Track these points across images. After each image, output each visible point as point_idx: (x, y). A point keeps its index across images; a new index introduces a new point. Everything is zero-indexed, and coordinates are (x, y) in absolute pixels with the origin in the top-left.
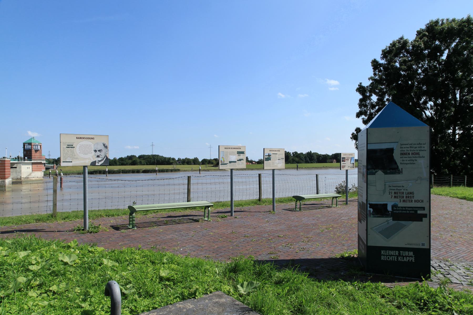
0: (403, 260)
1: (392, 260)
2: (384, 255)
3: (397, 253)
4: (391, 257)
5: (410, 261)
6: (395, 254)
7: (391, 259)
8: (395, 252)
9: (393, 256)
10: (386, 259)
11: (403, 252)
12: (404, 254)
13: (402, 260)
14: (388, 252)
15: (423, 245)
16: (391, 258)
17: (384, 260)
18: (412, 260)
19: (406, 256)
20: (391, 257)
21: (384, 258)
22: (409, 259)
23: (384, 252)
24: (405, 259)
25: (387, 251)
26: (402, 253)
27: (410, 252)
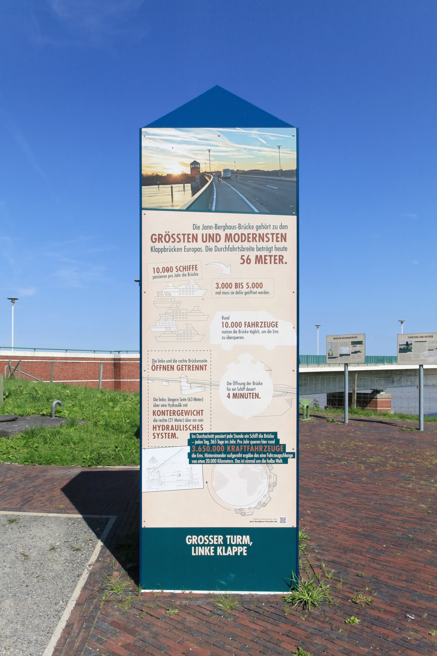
0: (226, 552)
3: (220, 539)
5: (239, 554)
6: (217, 541)
8: (217, 538)
11: (232, 536)
12: (234, 541)
13: (224, 554)
15: (283, 520)
18: (242, 553)
19: (237, 545)
22: (236, 551)
24: (230, 552)
26: (230, 538)
27: (244, 537)
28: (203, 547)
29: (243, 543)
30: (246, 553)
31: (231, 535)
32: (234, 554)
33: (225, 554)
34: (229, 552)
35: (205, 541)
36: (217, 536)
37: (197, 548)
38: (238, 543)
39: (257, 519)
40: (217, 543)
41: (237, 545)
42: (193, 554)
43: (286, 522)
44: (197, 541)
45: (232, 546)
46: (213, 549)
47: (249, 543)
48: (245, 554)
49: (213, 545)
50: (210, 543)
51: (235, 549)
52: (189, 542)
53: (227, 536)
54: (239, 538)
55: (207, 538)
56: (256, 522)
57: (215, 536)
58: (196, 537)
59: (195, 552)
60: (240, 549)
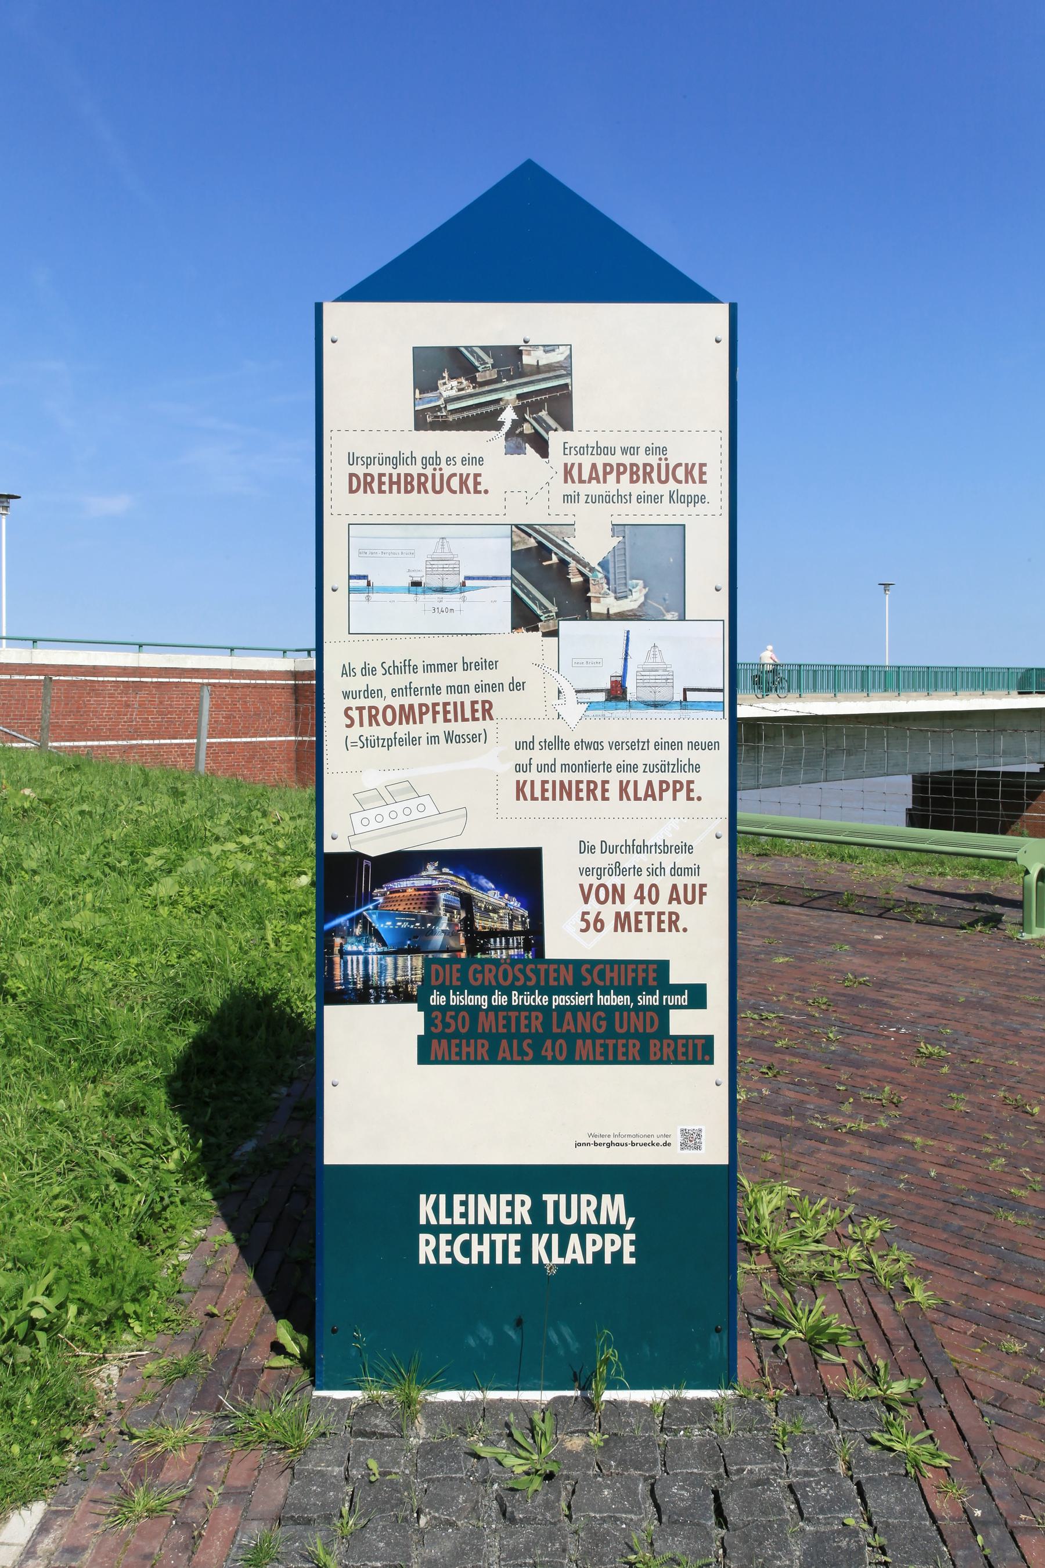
0: (562, 1253)
1: (486, 1260)
2: (436, 1230)
3: (523, 1207)
4: (481, 1242)
5: (608, 1260)
6: (511, 1215)
7: (481, 1255)
8: (512, 1203)
9: (499, 1228)
10: (450, 1254)
11: (563, 1197)
12: (568, 1215)
13: (557, 1260)
14: (464, 1203)
16: (480, 1249)
17: (438, 1265)
18: (618, 1255)
19: (583, 1230)
20: (481, 1242)
21: (436, 1252)
23: (436, 1208)
24: (575, 1254)
25: (458, 1198)
26: (556, 1204)
27: (606, 1198)
29: (603, 1221)
30: (632, 1255)
32: (590, 1260)
33: (561, 1261)
34: (574, 1252)
36: (509, 1197)
38: (584, 1221)
46: (517, 1243)
47: (623, 1221)
48: (628, 1260)
51: (594, 1243)
53: (545, 1197)
54: (589, 1203)
60: (613, 1243)
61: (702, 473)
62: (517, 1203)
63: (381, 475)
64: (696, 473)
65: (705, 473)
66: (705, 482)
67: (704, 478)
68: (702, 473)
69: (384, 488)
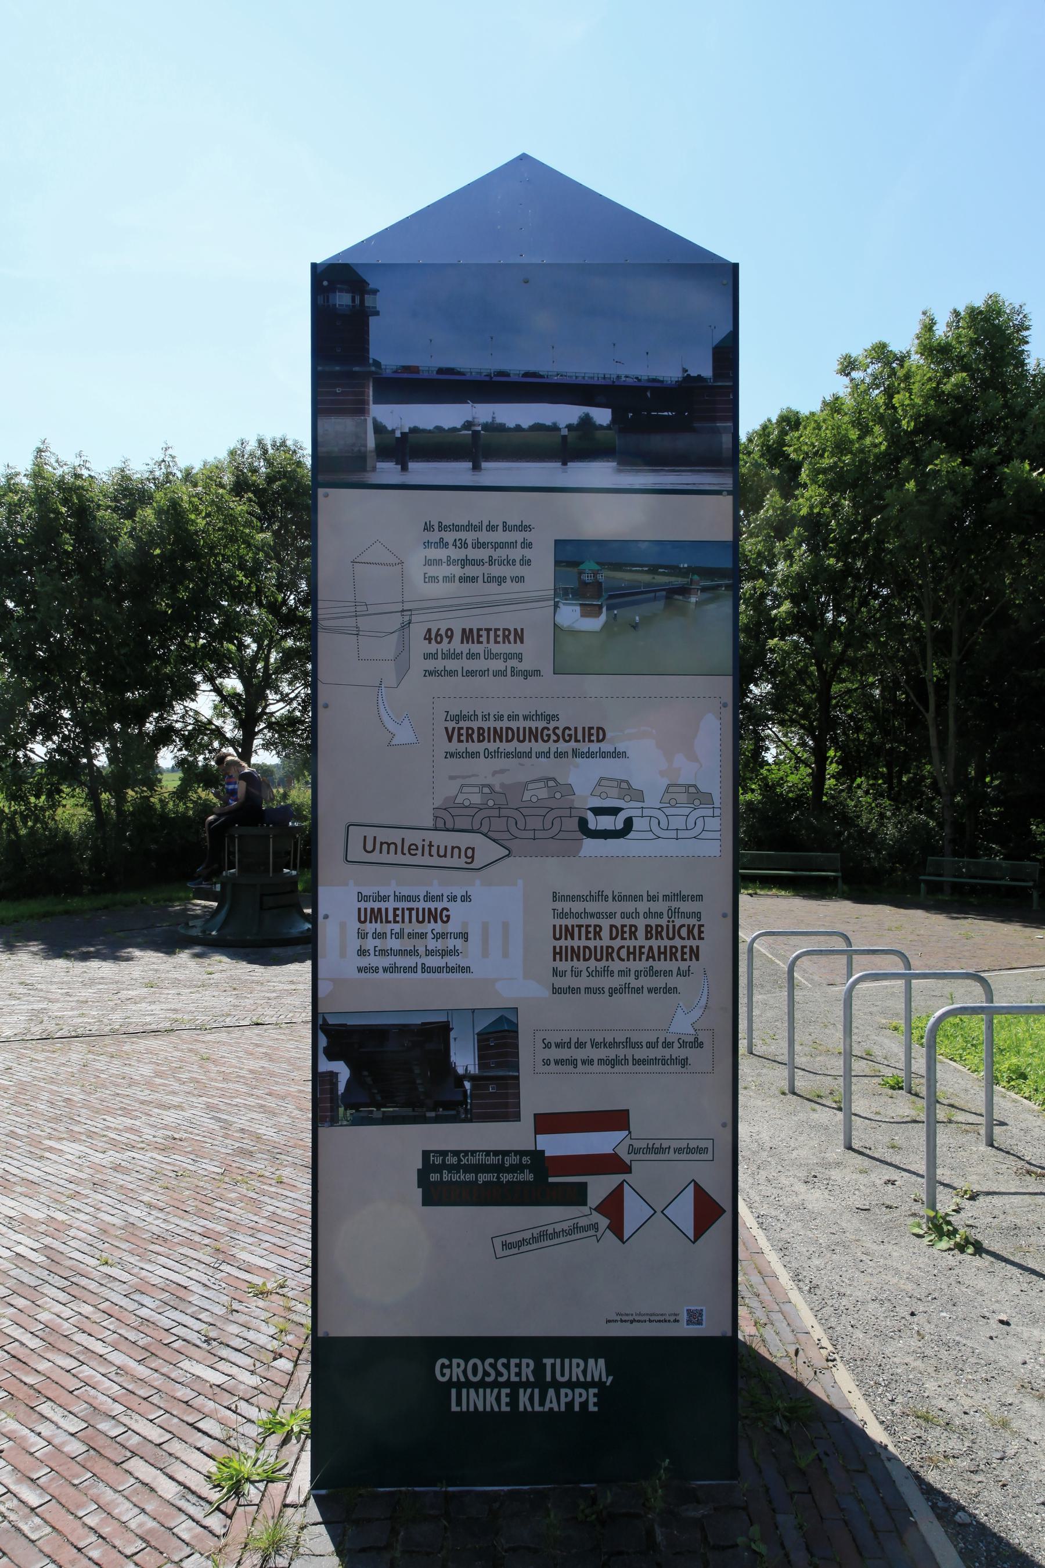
0: (542, 1403)
5: (577, 1408)
6: (519, 1374)
8: (519, 1365)
11: (558, 1361)
12: (563, 1375)
15: (695, 1317)
18: (584, 1405)
19: (571, 1385)
24: (552, 1403)
26: (553, 1366)
27: (591, 1362)
28: (481, 1391)
29: (589, 1379)
30: (595, 1404)
31: (555, 1358)
32: (563, 1409)
33: (541, 1409)
34: (551, 1402)
35: (486, 1374)
36: (517, 1361)
37: (464, 1391)
39: (627, 1315)
40: (517, 1379)
41: (571, 1385)
42: (454, 1408)
43: (704, 1323)
44: (465, 1372)
45: (557, 1386)
46: (507, 1395)
47: (604, 1379)
48: (592, 1408)
49: (508, 1384)
50: (501, 1379)
51: (566, 1395)
52: (443, 1375)
53: (545, 1361)
54: (578, 1365)
55: (491, 1365)
56: (622, 1321)
57: (514, 1361)
58: (462, 1362)
59: (459, 1403)
60: (581, 1395)
61: (700, 932)
62: (524, 1366)
63: (683, 947)
64: (696, 932)
65: (703, 932)
66: (703, 939)
67: (702, 935)
68: (700, 932)
69: (685, 957)
